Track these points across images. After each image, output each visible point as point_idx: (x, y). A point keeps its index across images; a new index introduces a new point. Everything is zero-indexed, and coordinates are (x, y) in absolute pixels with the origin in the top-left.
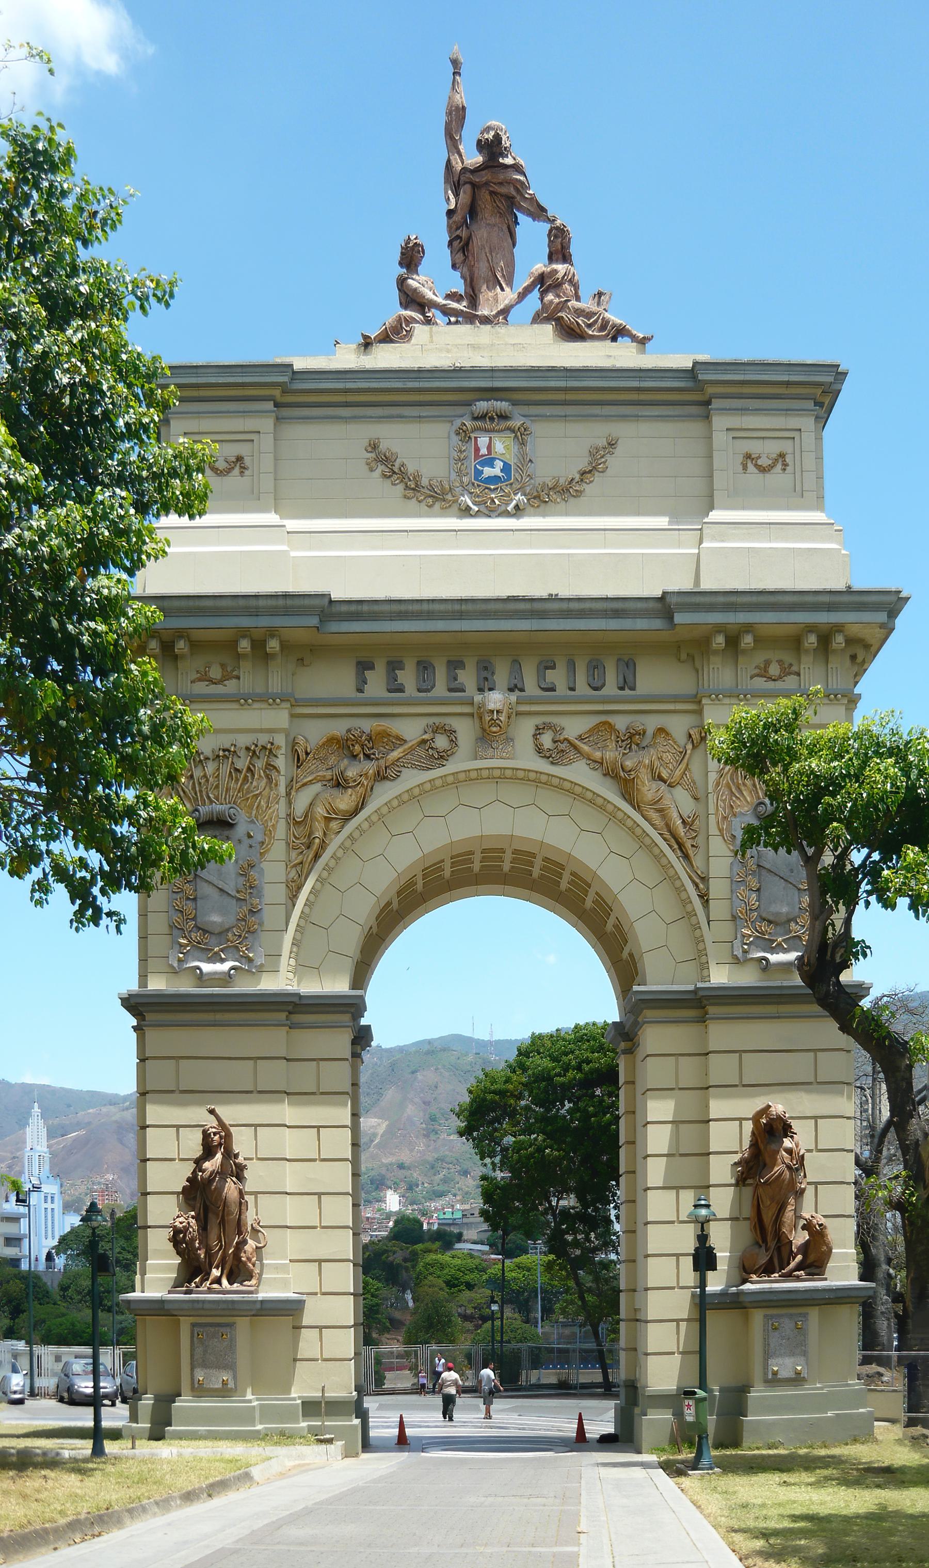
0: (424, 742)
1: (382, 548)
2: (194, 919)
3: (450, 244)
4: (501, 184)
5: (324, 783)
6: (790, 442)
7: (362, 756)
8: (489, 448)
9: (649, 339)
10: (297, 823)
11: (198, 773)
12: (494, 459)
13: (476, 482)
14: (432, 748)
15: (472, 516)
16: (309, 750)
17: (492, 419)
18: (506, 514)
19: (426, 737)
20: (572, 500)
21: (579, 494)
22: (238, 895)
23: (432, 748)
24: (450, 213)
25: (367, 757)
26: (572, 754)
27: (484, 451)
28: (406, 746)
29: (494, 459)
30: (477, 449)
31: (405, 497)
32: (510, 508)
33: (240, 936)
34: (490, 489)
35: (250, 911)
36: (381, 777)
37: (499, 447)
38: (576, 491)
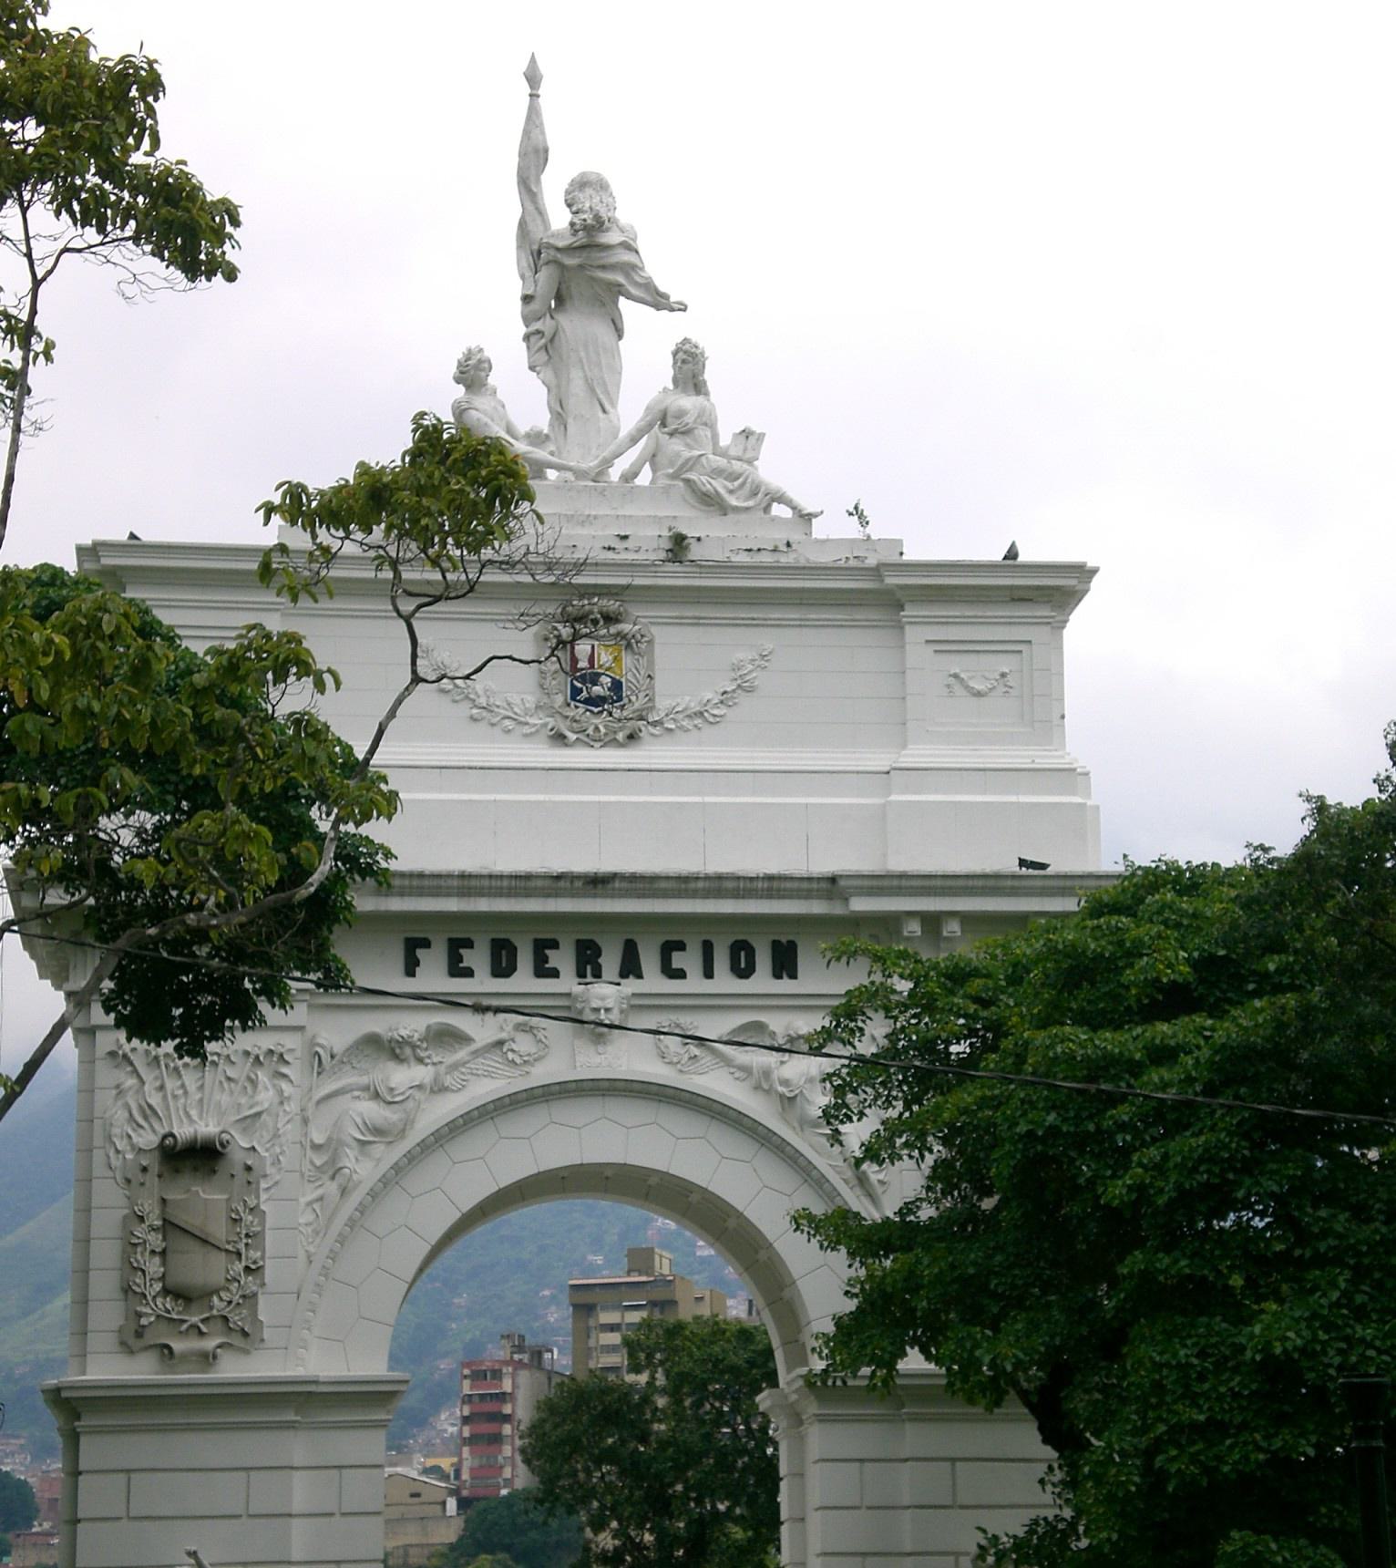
0: (500, 1043)
1: (441, 790)
2: (163, 1278)
3: (527, 338)
4: (603, 267)
5: (356, 1093)
6: (1013, 658)
7: (412, 1059)
8: (591, 660)
9: (816, 516)
10: (316, 1148)
11: (171, 1084)
12: (599, 675)
13: (573, 703)
14: (513, 1051)
15: (566, 745)
16: (335, 1051)
17: (595, 622)
18: (614, 743)
19: (504, 1035)
20: (707, 730)
21: (717, 721)
22: (228, 1247)
23: (513, 1051)
24: (527, 299)
25: (420, 1061)
26: (707, 1059)
27: (583, 664)
28: (474, 1047)
29: (599, 675)
30: (574, 660)
31: (473, 719)
32: (620, 736)
33: (230, 1302)
34: (591, 712)
35: (247, 1269)
36: (439, 1089)
37: (604, 657)
38: (714, 716)
